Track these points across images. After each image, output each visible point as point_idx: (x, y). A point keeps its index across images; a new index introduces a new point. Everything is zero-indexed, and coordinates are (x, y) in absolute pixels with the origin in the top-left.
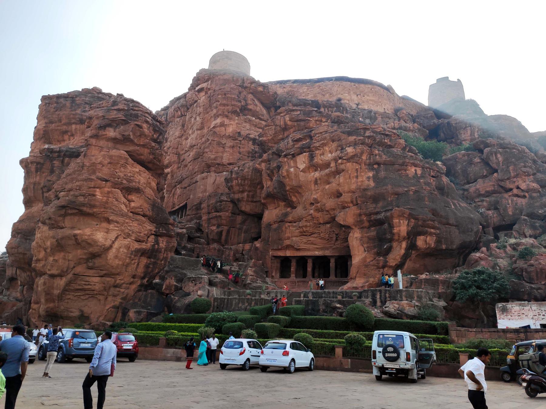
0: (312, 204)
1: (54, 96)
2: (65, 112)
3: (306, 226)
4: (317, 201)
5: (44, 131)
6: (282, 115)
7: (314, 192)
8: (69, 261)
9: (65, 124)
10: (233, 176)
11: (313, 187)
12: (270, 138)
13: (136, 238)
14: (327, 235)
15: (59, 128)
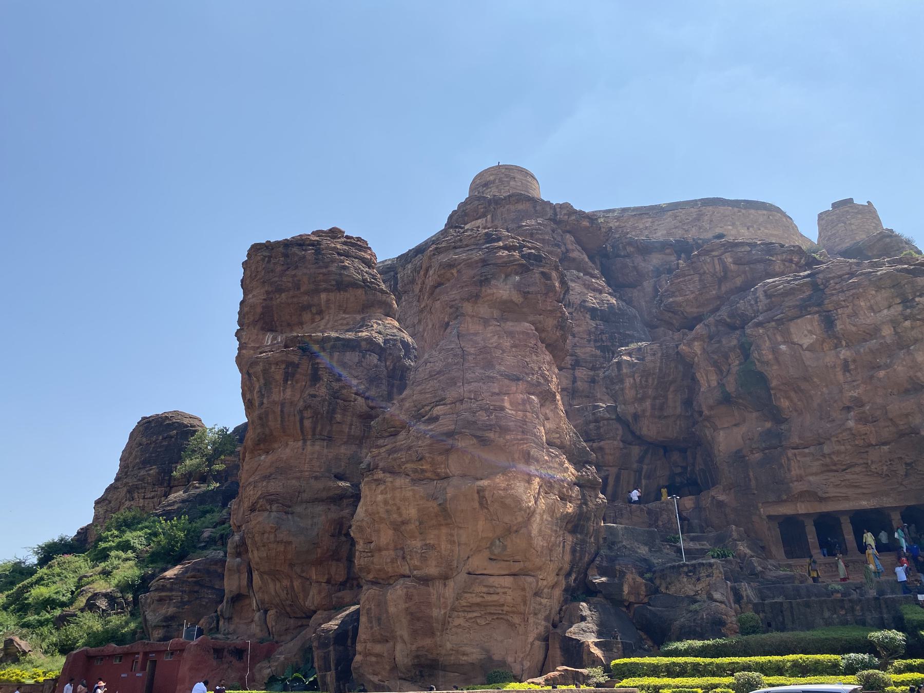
0: (848, 409)
1: (278, 243)
2: (305, 271)
3: (838, 453)
4: (859, 403)
5: (263, 307)
6: (714, 253)
7: (846, 387)
8: (459, 545)
9: (306, 293)
10: (625, 371)
11: (840, 377)
12: (692, 296)
13: (560, 492)
14: (885, 468)
15: (295, 300)
